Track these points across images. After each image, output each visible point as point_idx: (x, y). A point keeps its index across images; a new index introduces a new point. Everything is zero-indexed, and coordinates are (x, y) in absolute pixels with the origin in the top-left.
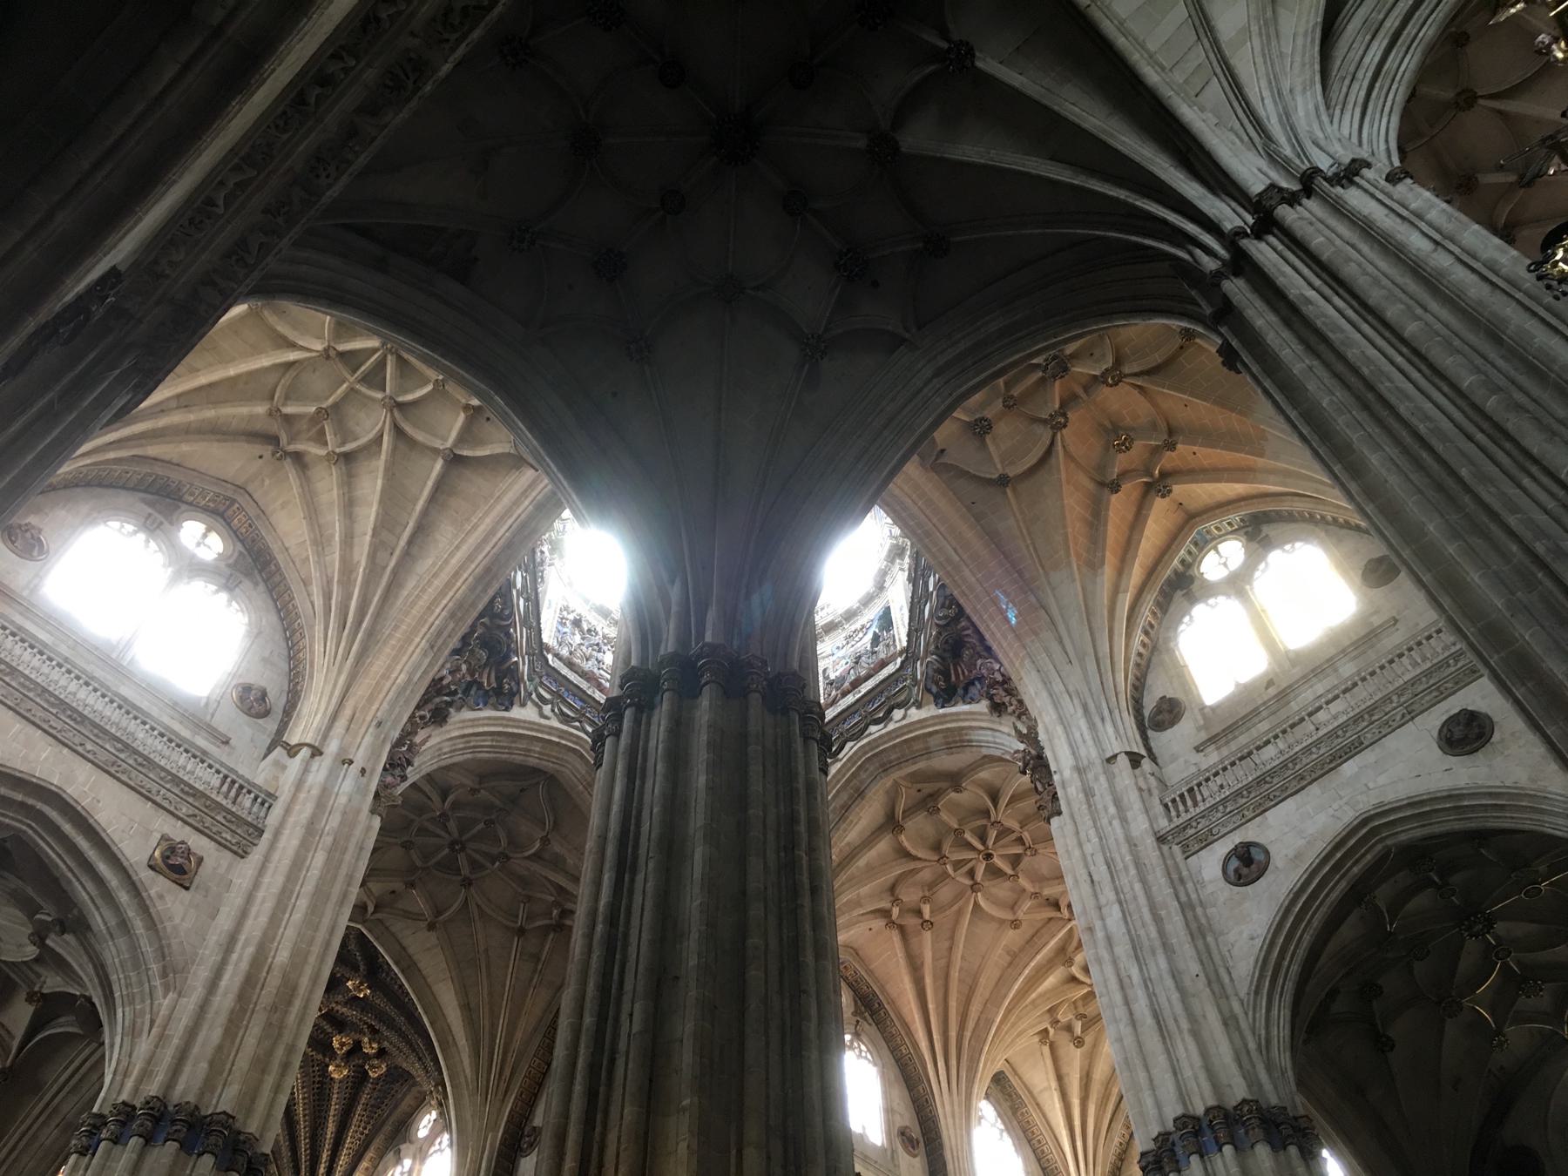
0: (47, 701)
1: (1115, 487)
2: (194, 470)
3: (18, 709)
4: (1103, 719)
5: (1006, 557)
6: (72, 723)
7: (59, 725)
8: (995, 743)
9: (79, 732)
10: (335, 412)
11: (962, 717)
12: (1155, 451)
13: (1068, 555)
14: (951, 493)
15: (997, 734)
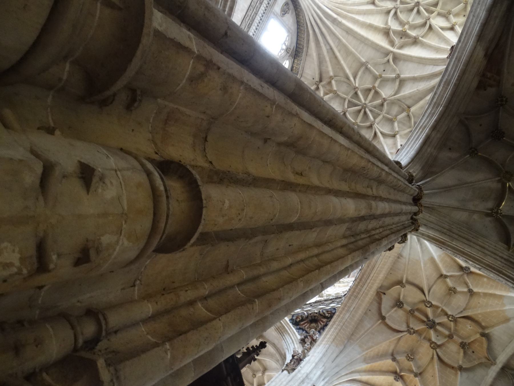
0: (254, 15)
1: (394, 359)
2: (306, 60)
3: (251, 6)
4: (323, 380)
5: (356, 328)
6: (248, 24)
7: (247, 20)
8: (289, 344)
9: (245, 27)
10: (336, 95)
11: (291, 330)
12: (411, 371)
13: (367, 349)
14: (371, 301)
15: (292, 344)
